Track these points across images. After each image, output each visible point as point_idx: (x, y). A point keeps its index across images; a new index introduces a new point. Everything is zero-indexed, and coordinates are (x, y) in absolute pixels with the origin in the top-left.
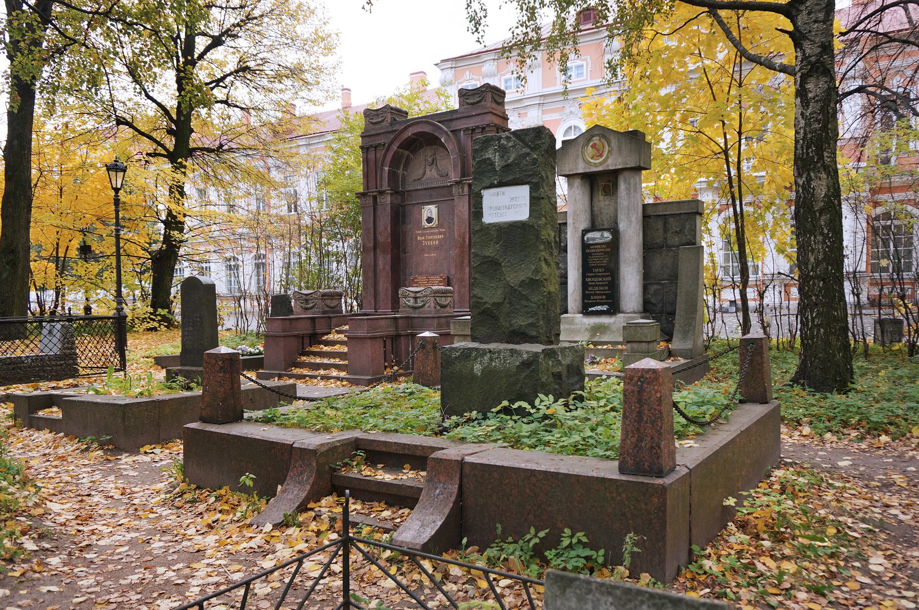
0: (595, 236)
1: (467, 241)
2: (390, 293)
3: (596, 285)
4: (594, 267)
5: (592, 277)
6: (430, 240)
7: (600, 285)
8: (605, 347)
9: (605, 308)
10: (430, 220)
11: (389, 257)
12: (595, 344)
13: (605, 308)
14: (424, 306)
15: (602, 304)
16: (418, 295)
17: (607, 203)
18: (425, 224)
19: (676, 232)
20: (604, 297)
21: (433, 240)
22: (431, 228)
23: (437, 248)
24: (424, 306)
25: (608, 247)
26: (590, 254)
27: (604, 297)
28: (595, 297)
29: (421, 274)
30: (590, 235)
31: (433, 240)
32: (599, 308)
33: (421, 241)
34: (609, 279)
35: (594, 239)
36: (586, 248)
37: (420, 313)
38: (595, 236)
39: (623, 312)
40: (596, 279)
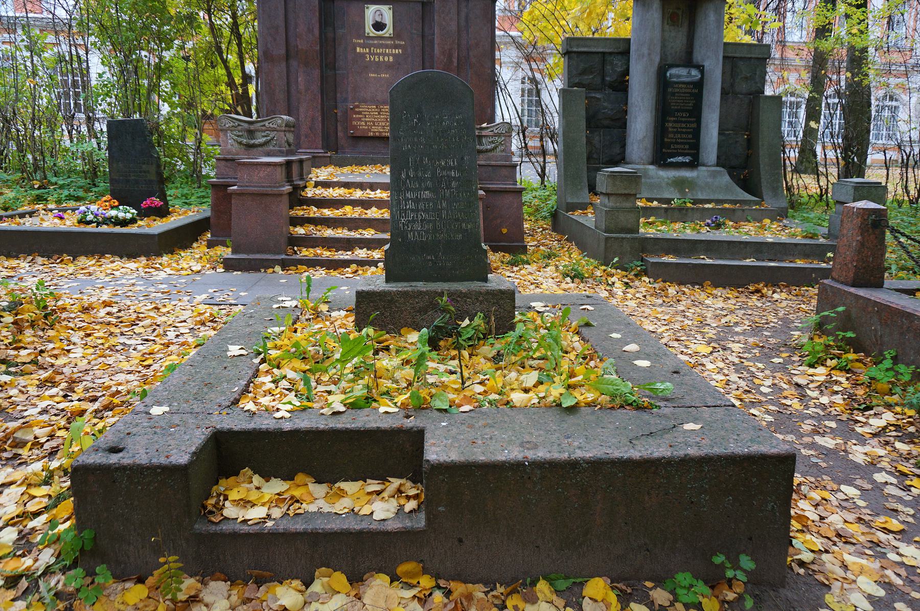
0: (679, 73)
1: (455, 61)
2: (319, 126)
3: (677, 132)
4: (678, 111)
6: (379, 55)
7: (682, 133)
8: (707, 206)
9: (687, 159)
10: (379, 26)
11: (317, 73)
12: (695, 202)
13: (687, 159)
14: (495, 148)
15: (684, 155)
16: (484, 133)
17: (673, 34)
18: (370, 30)
19: (746, 78)
20: (687, 147)
21: (384, 55)
22: (381, 38)
23: (389, 67)
24: (495, 148)
25: (695, 87)
27: (687, 147)
28: (677, 146)
29: (365, 101)
30: (674, 71)
31: (384, 55)
33: (363, 55)
34: (694, 125)
35: (679, 76)
36: (663, 84)
37: (489, 159)
38: (679, 73)
39: (704, 165)
40: (678, 125)
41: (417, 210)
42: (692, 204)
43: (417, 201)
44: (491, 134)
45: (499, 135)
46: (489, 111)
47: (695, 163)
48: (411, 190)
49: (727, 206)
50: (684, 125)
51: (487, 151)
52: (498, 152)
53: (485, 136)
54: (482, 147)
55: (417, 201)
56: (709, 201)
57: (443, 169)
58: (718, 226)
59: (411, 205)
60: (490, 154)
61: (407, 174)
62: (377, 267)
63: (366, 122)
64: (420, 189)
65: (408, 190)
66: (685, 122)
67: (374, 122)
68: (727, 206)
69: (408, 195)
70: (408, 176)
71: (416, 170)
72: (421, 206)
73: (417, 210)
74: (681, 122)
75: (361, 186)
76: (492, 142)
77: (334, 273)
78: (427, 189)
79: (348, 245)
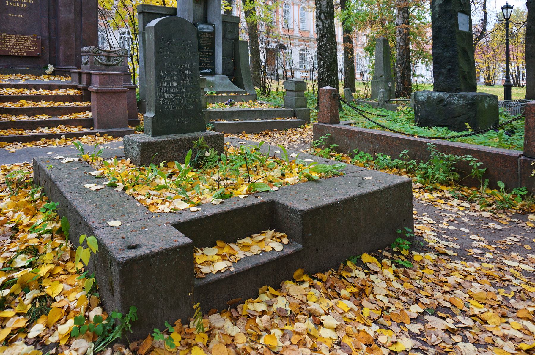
3: (204, 57)
5: (202, 52)
7: (206, 57)
8: (223, 95)
9: (209, 71)
12: (218, 93)
13: (209, 71)
14: (118, 63)
15: (208, 69)
16: (111, 54)
20: (209, 65)
24: (118, 63)
26: (201, 38)
27: (209, 65)
32: (206, 71)
34: (212, 54)
35: (203, 29)
39: (217, 74)
40: (205, 53)
41: (169, 93)
42: (216, 94)
43: (169, 87)
44: (116, 55)
45: (120, 56)
46: (95, 42)
47: (213, 74)
48: (167, 81)
49: (232, 94)
50: (207, 54)
51: (114, 65)
52: (120, 66)
53: (112, 56)
54: (110, 63)
55: (169, 87)
56: (224, 92)
57: (183, 69)
58: (232, 104)
59: (166, 90)
60: (115, 67)
61: (164, 72)
62: (60, 138)
63: (7, 45)
64: (171, 81)
65: (165, 81)
66: (207, 52)
67: (13, 46)
68: (232, 94)
69: (165, 85)
70: (164, 74)
71: (168, 70)
72: (172, 90)
73: (169, 93)
74: (206, 52)
75: (28, 87)
76: (117, 60)
77: (29, 145)
78: (175, 81)
79: (55, 124)
